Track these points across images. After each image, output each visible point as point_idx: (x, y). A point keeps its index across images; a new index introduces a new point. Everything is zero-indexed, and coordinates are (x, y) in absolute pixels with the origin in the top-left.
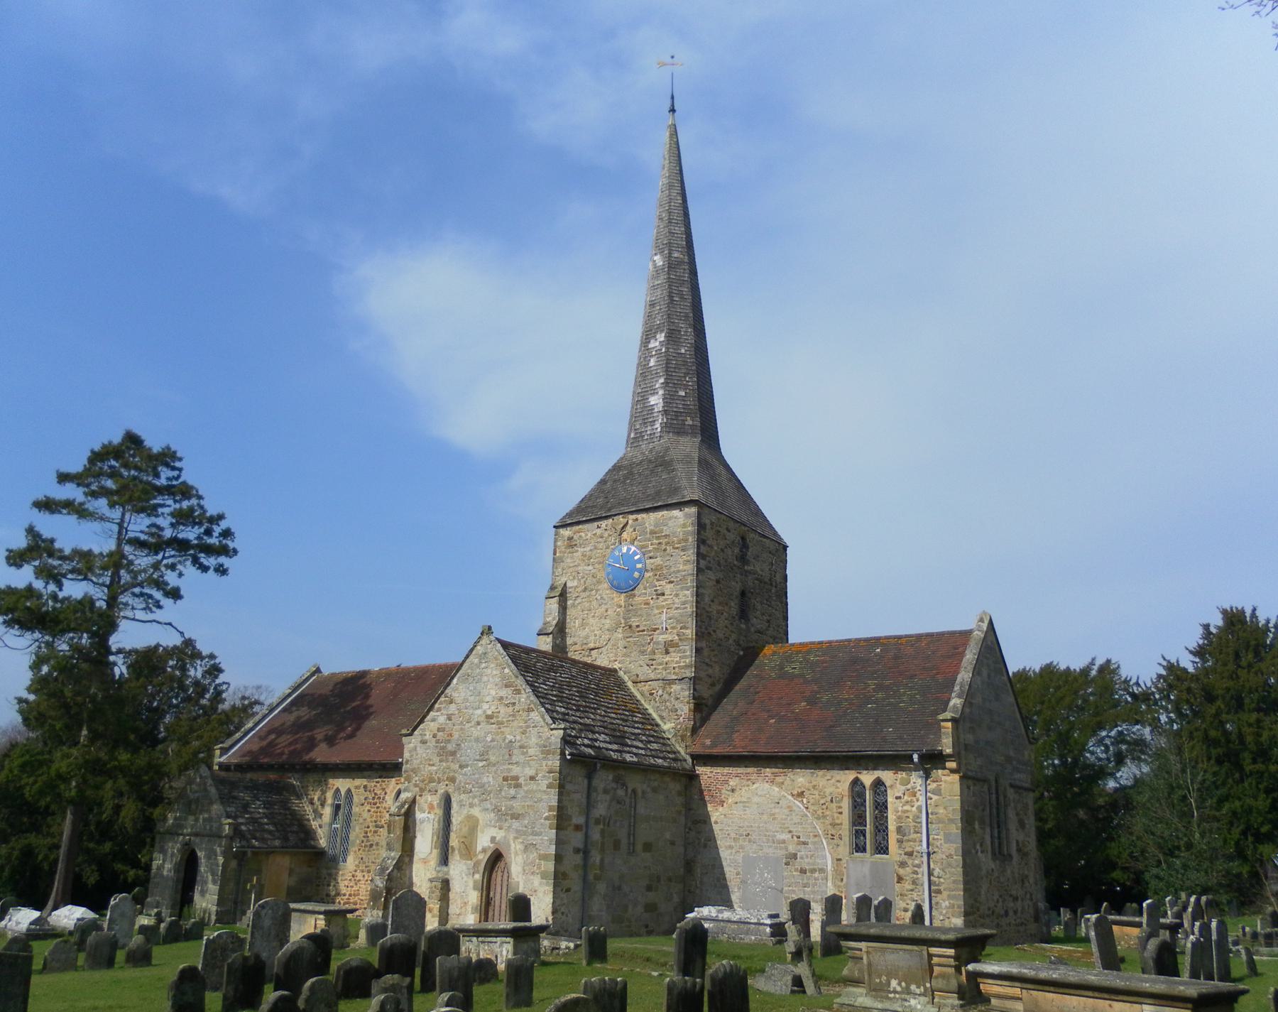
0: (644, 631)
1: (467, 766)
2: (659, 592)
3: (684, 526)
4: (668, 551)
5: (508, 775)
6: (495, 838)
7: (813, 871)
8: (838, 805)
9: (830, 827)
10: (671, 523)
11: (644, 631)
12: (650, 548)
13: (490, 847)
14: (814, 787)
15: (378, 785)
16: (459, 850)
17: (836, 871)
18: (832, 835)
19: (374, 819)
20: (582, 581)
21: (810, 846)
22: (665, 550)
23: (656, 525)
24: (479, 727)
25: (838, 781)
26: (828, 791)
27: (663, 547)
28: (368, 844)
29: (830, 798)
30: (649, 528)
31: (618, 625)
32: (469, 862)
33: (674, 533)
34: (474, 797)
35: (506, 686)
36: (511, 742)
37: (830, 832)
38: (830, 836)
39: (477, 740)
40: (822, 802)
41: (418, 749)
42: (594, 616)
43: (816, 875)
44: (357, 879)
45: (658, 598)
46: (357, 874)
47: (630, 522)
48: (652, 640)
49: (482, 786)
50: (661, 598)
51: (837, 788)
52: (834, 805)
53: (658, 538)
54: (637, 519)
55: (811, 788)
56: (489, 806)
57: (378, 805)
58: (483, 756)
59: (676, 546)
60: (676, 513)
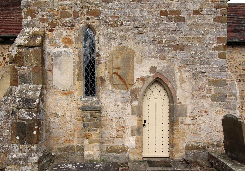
7: (230, 96)
8: (243, 66)
9: (238, 76)
14: (231, 58)
17: (241, 95)
18: (239, 80)
21: (229, 85)
25: (243, 56)
26: (238, 60)
29: (239, 63)
37: (238, 79)
38: (238, 80)
40: (235, 65)
43: (232, 98)
51: (243, 59)
52: (241, 67)
55: (230, 59)
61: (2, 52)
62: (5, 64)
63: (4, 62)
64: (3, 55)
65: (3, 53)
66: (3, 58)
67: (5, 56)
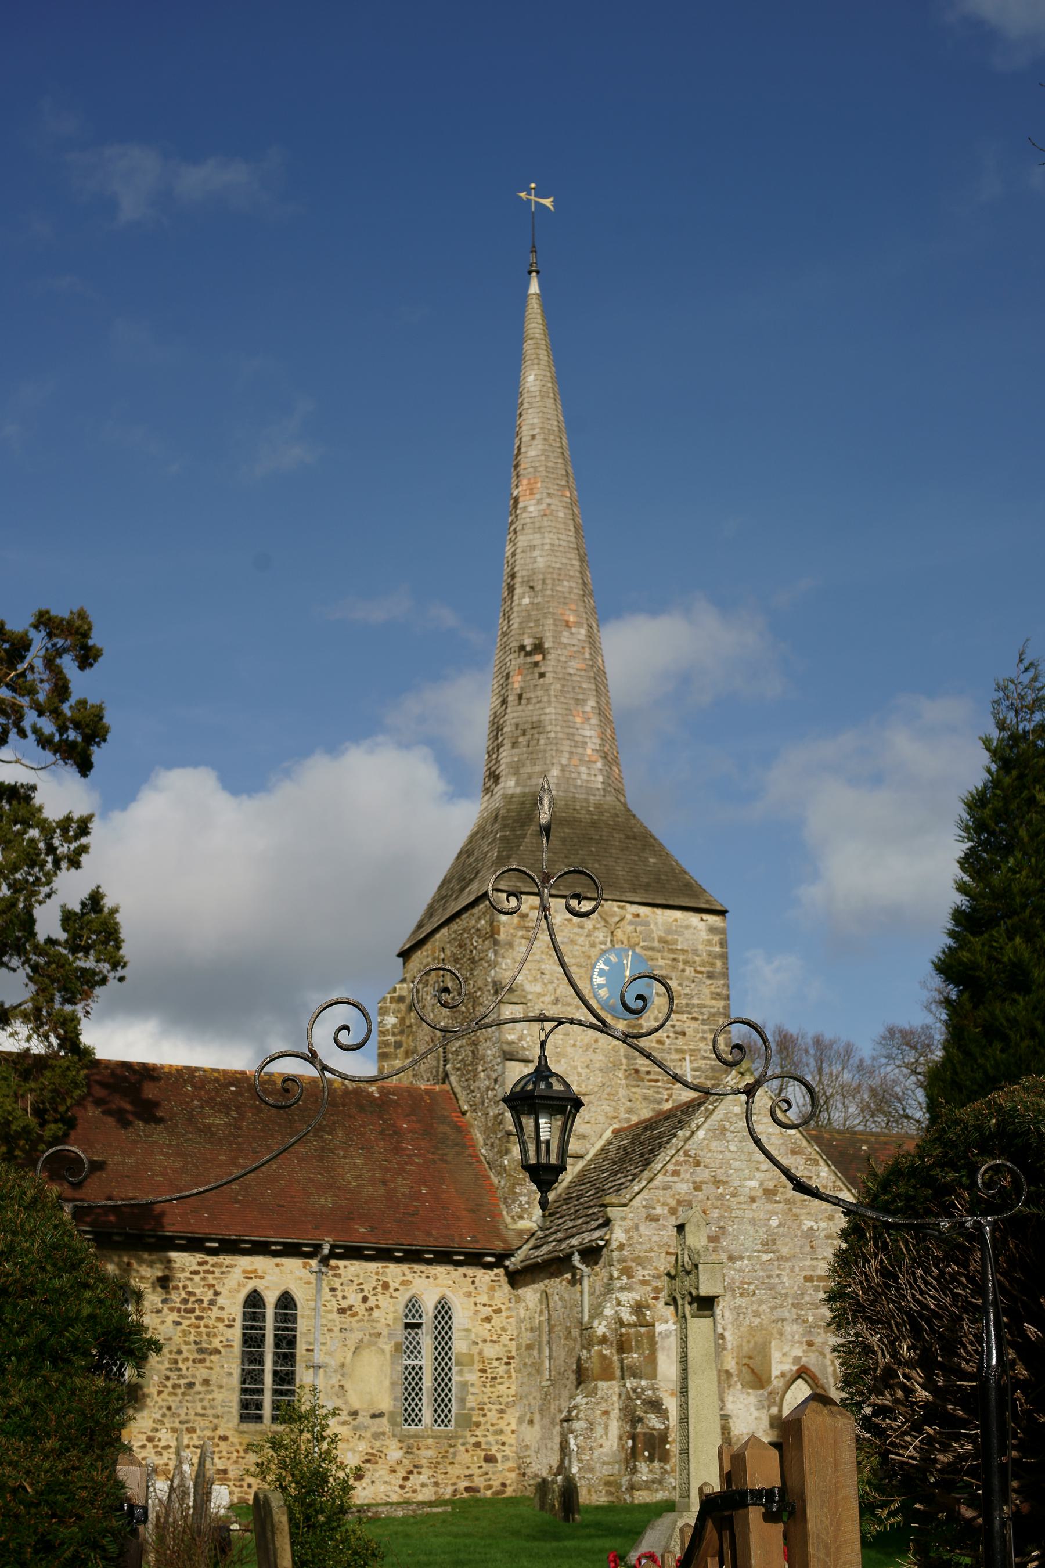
0: (657, 1081)
1: (741, 1258)
2: (677, 1029)
3: (709, 942)
4: (687, 973)
5: (811, 1273)
6: (800, 1358)
10: (688, 934)
11: (657, 1081)
12: (661, 962)
13: (791, 1370)
15: (197, 1278)
16: (738, 1376)
19: (192, 1338)
20: (550, 987)
22: (683, 971)
23: (669, 931)
24: (754, 1206)
27: (681, 966)
28: (182, 1382)
30: (658, 932)
31: (616, 1066)
32: (761, 1391)
33: (695, 952)
34: (761, 1302)
35: (794, 1152)
36: (811, 1229)
39: (753, 1222)
41: (642, 1228)
42: (574, 1045)
44: (162, 1444)
45: (676, 1038)
46: (158, 1435)
47: (629, 917)
48: (670, 1096)
49: (772, 1288)
50: (680, 1041)
53: (672, 951)
54: (638, 916)
56: (787, 1315)
57: (198, 1313)
58: (769, 1244)
59: (699, 969)
60: (694, 919)
61: (361, 1281)
62: (367, 1314)
63: (363, 1306)
64: (362, 1290)
65: (362, 1284)
66: (361, 1295)
67: (366, 1293)
